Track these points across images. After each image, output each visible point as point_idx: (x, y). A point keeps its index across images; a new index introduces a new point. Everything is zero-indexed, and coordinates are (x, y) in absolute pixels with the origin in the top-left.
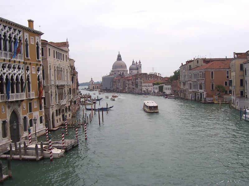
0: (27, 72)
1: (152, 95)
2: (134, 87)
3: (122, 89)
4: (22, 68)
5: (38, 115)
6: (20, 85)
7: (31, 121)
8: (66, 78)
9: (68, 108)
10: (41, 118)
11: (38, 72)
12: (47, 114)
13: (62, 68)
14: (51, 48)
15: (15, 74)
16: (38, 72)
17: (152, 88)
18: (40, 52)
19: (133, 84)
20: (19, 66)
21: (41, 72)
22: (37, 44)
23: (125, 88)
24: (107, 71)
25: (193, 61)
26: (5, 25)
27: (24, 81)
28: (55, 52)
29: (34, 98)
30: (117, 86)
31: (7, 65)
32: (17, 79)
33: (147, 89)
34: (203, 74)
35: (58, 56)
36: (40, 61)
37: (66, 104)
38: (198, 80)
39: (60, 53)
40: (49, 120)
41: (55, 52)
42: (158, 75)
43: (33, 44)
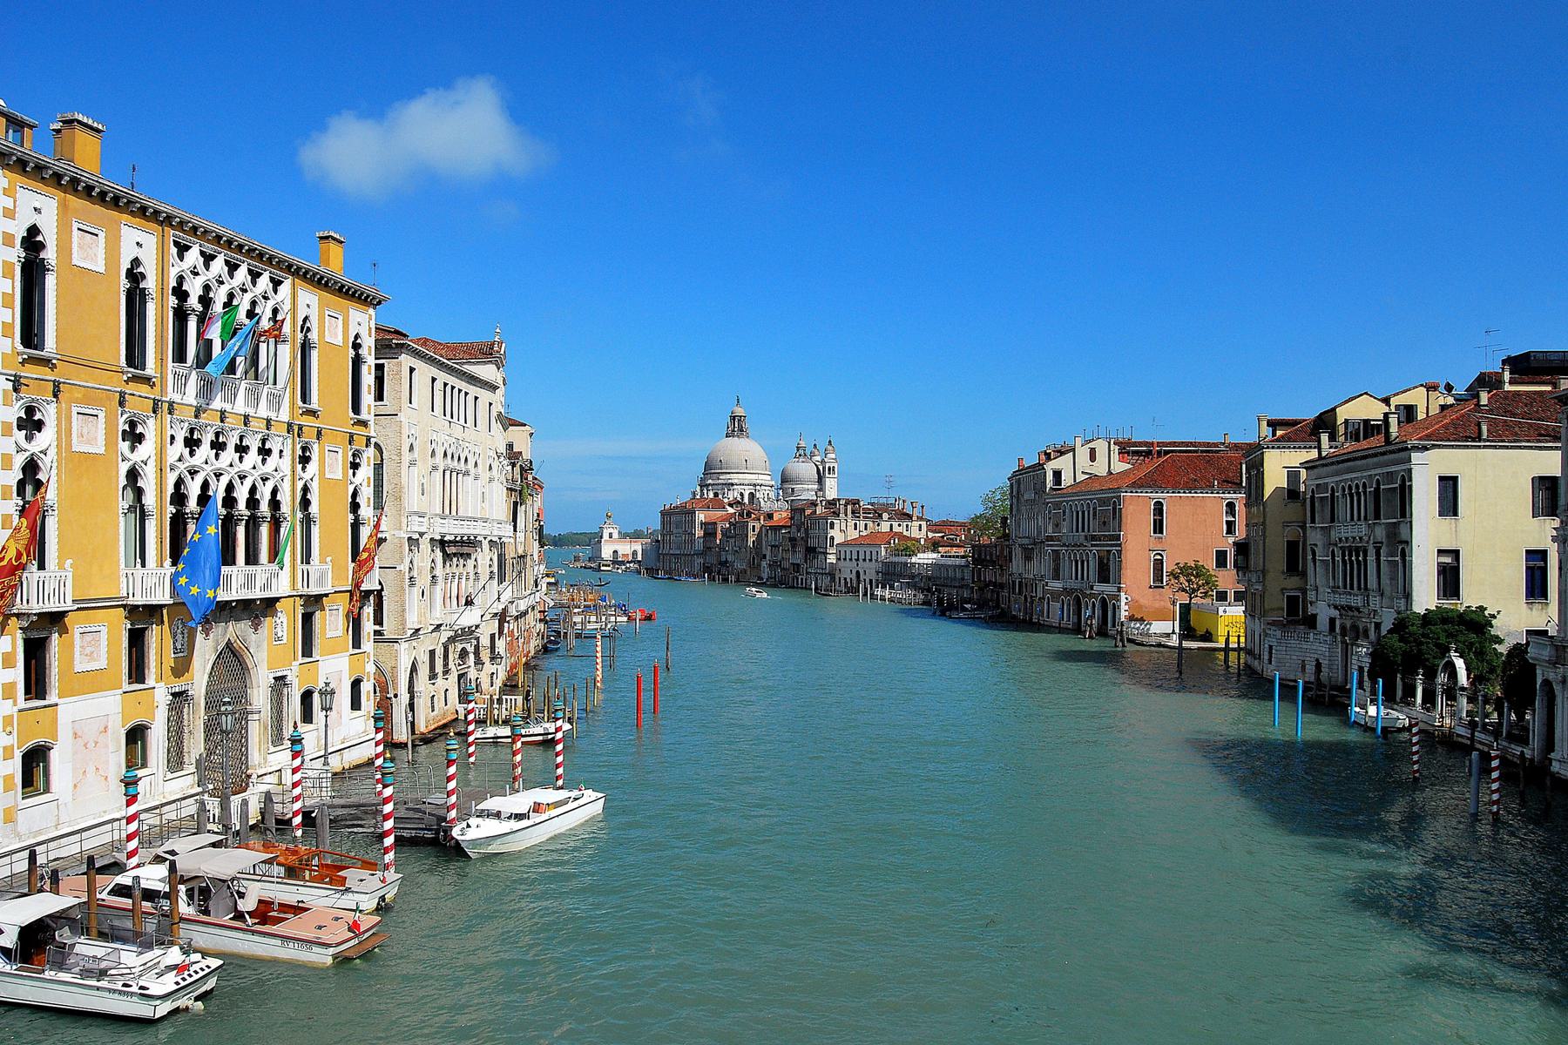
0: (304, 469)
4: (281, 451)
6: (264, 530)
7: (307, 697)
9: (485, 641)
10: (356, 684)
11: (354, 475)
15: (242, 478)
16: (354, 475)
18: (368, 379)
19: (794, 546)
20: (264, 441)
21: (366, 472)
22: (356, 346)
23: (759, 565)
26: (209, 252)
27: (285, 508)
28: (439, 385)
29: (328, 589)
31: (208, 438)
32: (253, 503)
33: (858, 572)
34: (1114, 509)
36: (364, 424)
37: (477, 627)
38: (1094, 538)
40: (396, 696)
41: (439, 385)
43: (339, 340)
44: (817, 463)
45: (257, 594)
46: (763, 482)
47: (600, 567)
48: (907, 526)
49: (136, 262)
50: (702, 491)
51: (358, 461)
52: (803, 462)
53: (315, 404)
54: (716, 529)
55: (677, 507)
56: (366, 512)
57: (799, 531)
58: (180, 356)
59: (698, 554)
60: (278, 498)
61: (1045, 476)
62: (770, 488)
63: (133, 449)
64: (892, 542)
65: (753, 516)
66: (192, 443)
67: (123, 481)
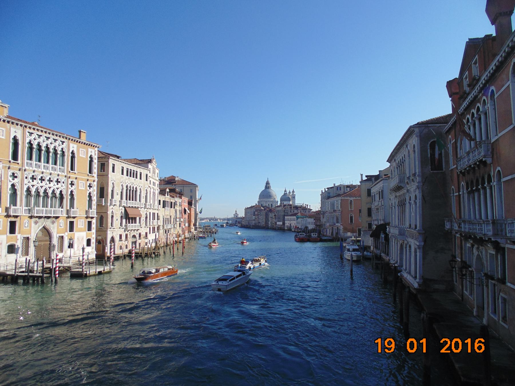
0: (72, 187)
1: (292, 232)
5: (83, 236)
8: (143, 200)
9: (143, 234)
11: (90, 189)
12: (103, 238)
13: (136, 188)
14: (116, 163)
16: (90, 189)
17: (295, 222)
22: (91, 157)
23: (268, 223)
24: (254, 201)
25: (333, 187)
26: (39, 134)
30: (259, 220)
35: (131, 174)
37: (138, 230)
39: (134, 171)
43: (85, 157)
45: (52, 215)
49: (15, 137)
51: (91, 185)
53: (76, 172)
55: (249, 208)
56: (95, 198)
58: (31, 158)
60: (63, 193)
63: (13, 179)
66: (33, 178)
67: (10, 187)
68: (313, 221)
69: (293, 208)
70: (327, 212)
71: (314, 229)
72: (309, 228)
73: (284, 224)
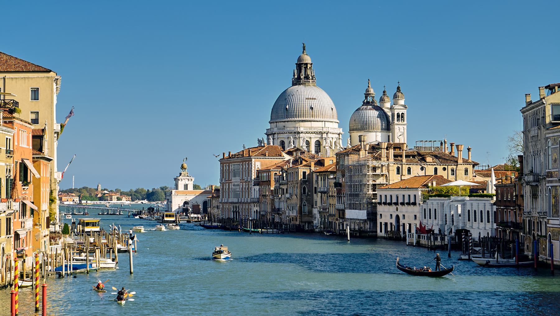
1: (411, 245)
2: (341, 207)
3: (295, 214)
17: (415, 210)
19: (339, 192)
23: (310, 213)
30: (276, 200)
33: (398, 217)
42: (455, 153)
44: (386, 110)
46: (330, 131)
47: (163, 218)
48: (452, 170)
50: (268, 139)
52: (370, 109)
54: (269, 176)
57: (343, 176)
59: (258, 202)
61: (544, 111)
62: (337, 136)
64: (430, 185)
65: (304, 163)
68: (488, 208)
69: (406, 156)
70: (550, 175)
71: (493, 239)
72: (475, 235)
73: (372, 216)
